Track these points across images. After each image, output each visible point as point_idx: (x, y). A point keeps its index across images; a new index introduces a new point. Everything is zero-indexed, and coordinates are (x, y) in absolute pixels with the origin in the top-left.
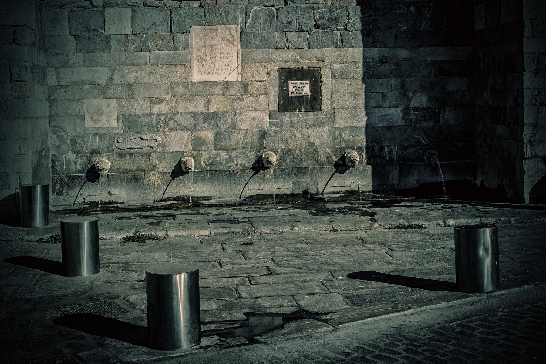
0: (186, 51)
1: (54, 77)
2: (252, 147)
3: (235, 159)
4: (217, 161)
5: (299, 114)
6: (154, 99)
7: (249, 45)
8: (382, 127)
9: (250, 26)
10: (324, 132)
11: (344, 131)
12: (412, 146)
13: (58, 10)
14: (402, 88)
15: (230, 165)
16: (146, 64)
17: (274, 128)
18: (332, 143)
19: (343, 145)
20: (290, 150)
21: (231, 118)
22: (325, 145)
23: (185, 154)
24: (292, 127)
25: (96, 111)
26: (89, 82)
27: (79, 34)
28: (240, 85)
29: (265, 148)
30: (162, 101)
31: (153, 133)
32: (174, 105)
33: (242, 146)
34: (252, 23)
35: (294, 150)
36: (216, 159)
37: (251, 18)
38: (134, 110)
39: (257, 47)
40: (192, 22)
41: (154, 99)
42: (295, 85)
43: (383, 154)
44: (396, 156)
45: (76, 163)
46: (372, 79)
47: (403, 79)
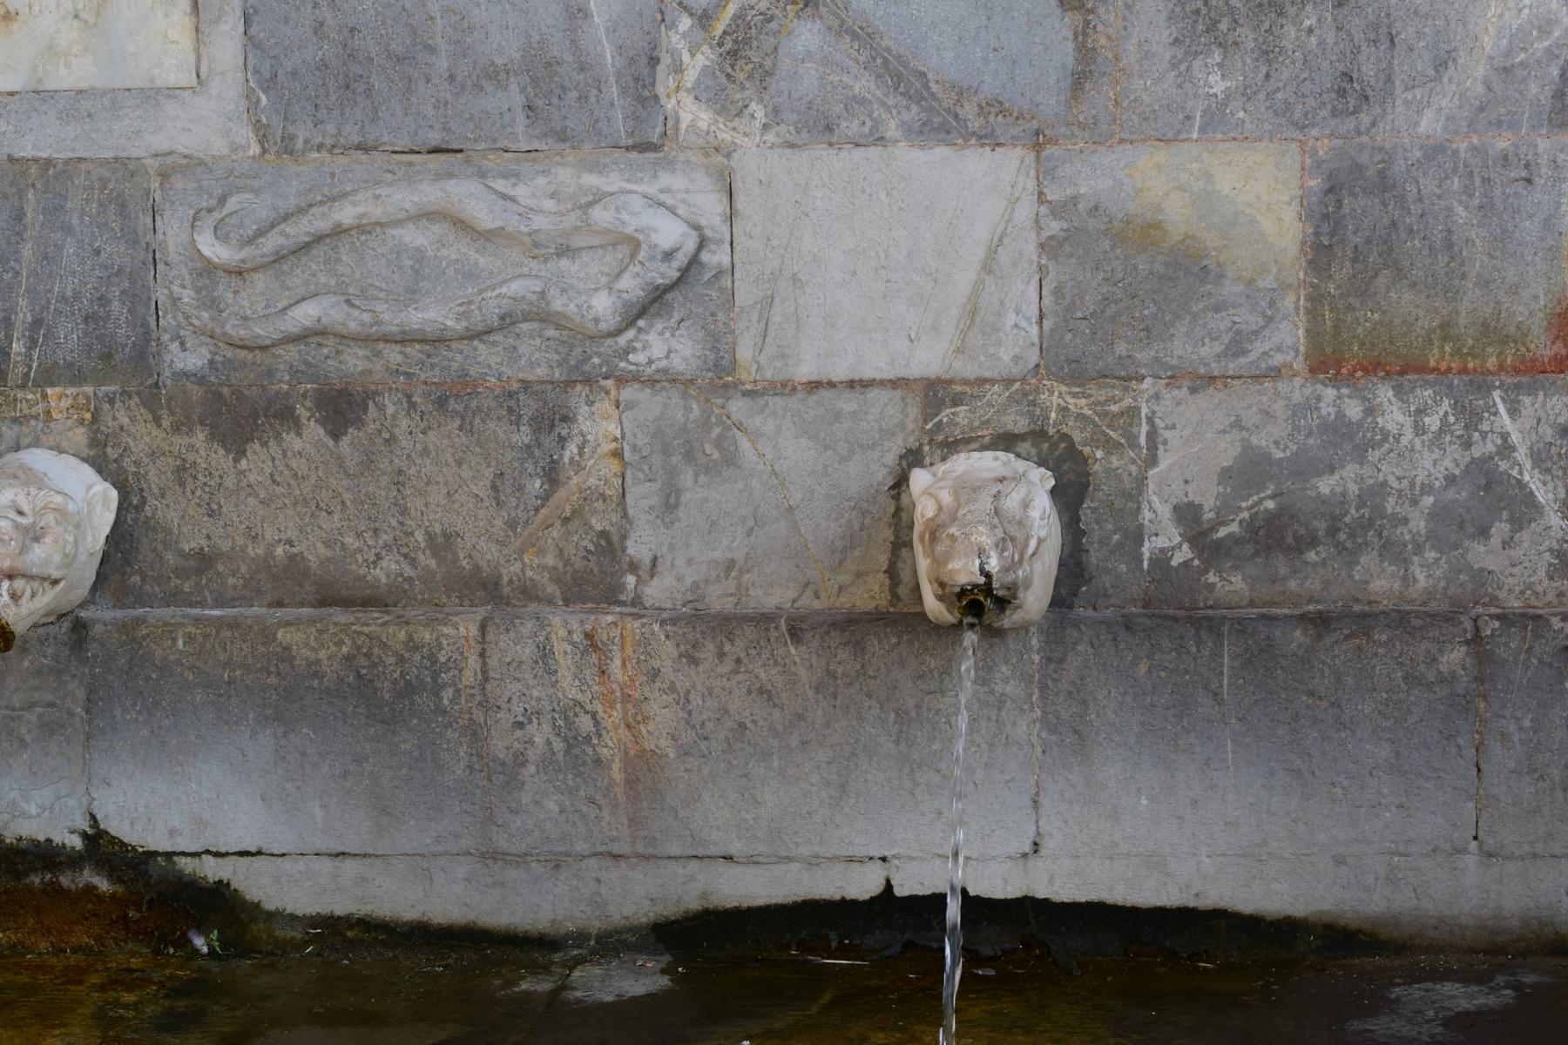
4: (1333, 511)
15: (1483, 555)
31: (597, 167)
36: (1325, 485)
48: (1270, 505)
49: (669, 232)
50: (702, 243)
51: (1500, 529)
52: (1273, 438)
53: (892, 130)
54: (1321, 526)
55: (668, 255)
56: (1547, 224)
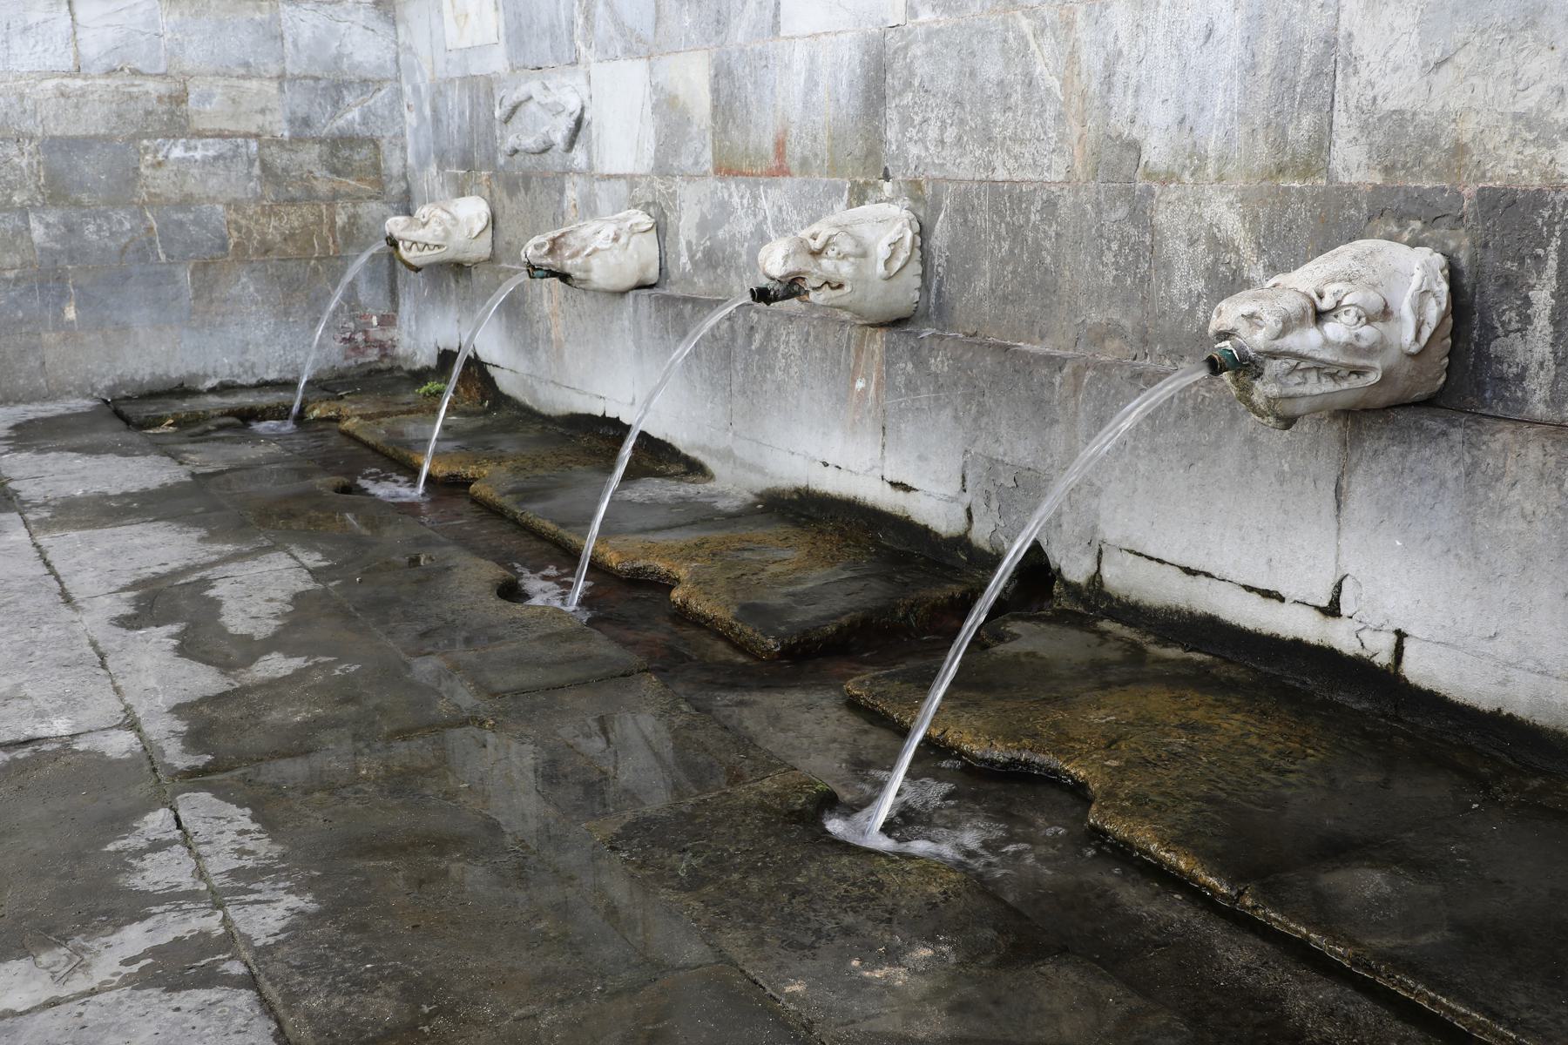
2: (835, 169)
10: (1209, 34)
18: (1263, 149)
29: (887, 177)
48: (708, 243)
49: (574, 105)
50: (583, 109)
53: (619, 54)
55: (571, 114)
56: (772, 92)
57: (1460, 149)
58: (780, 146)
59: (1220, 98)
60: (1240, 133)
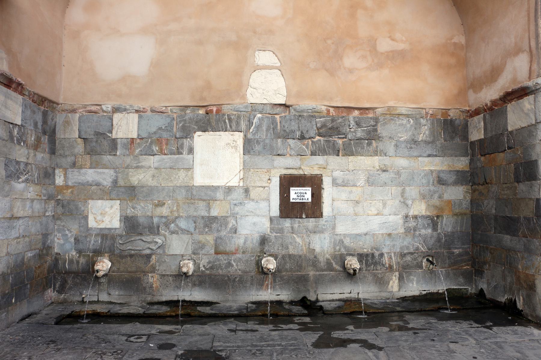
0: (189, 156)
1: (62, 178)
3: (235, 264)
5: (300, 220)
6: (156, 202)
7: (252, 151)
8: (382, 234)
9: (254, 132)
11: (345, 237)
12: (412, 254)
13: (69, 115)
14: (402, 196)
15: (229, 270)
16: (150, 167)
17: (275, 234)
19: (343, 251)
20: (290, 256)
21: (232, 222)
22: (326, 252)
23: (185, 258)
24: (293, 233)
25: (100, 212)
26: (94, 184)
27: (88, 137)
28: (242, 191)
29: (265, 254)
30: (164, 204)
31: (154, 236)
32: (175, 208)
33: (242, 251)
34: (255, 130)
35: (295, 256)
37: (254, 125)
38: (136, 212)
39: (259, 154)
40: (196, 127)
41: (156, 202)
42: (297, 192)
43: (383, 261)
44: (396, 263)
45: (78, 262)
46: (373, 187)
47: (403, 187)
51: (231, 267)
52: (211, 260)
54: (215, 267)
55: (160, 243)
57: (355, 250)
58: (237, 250)
59: (327, 245)
60: (330, 248)
